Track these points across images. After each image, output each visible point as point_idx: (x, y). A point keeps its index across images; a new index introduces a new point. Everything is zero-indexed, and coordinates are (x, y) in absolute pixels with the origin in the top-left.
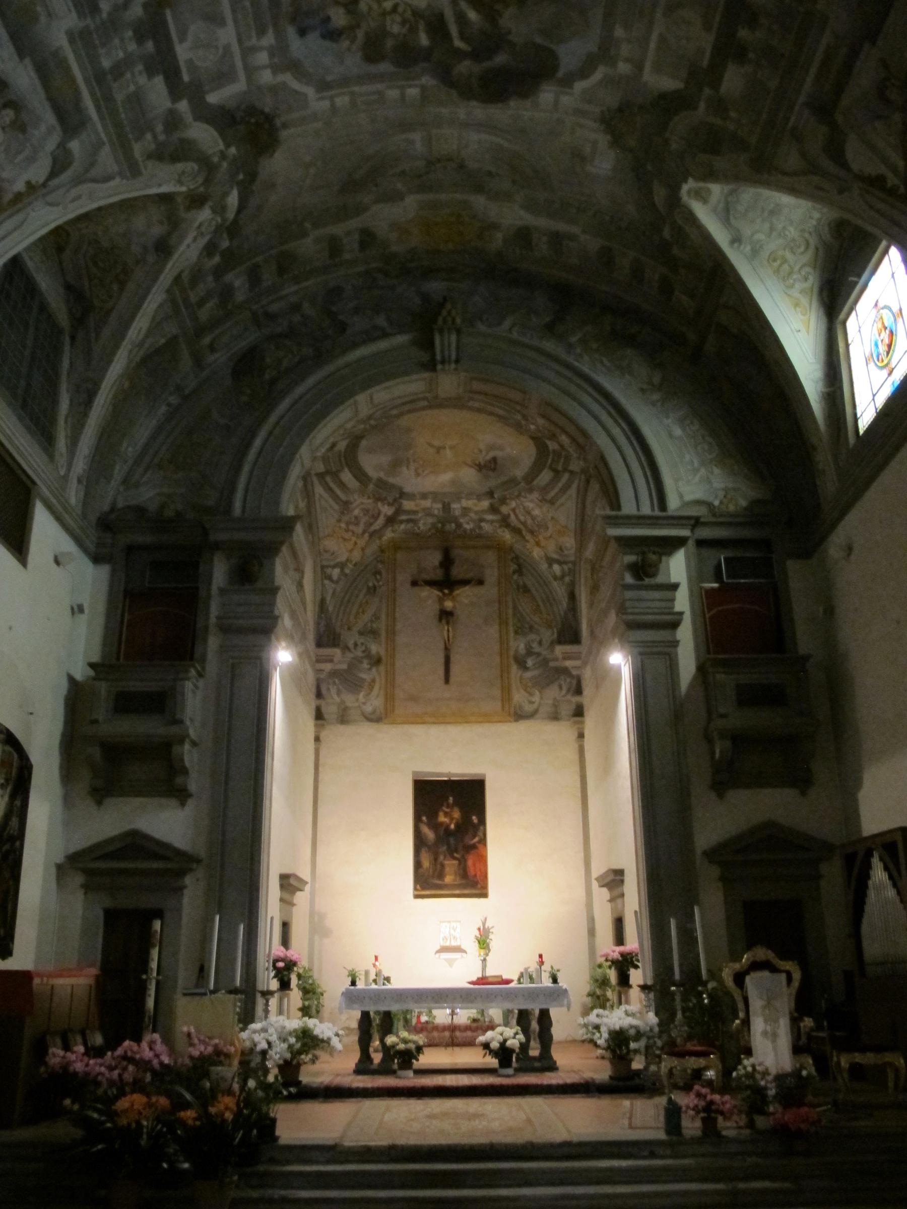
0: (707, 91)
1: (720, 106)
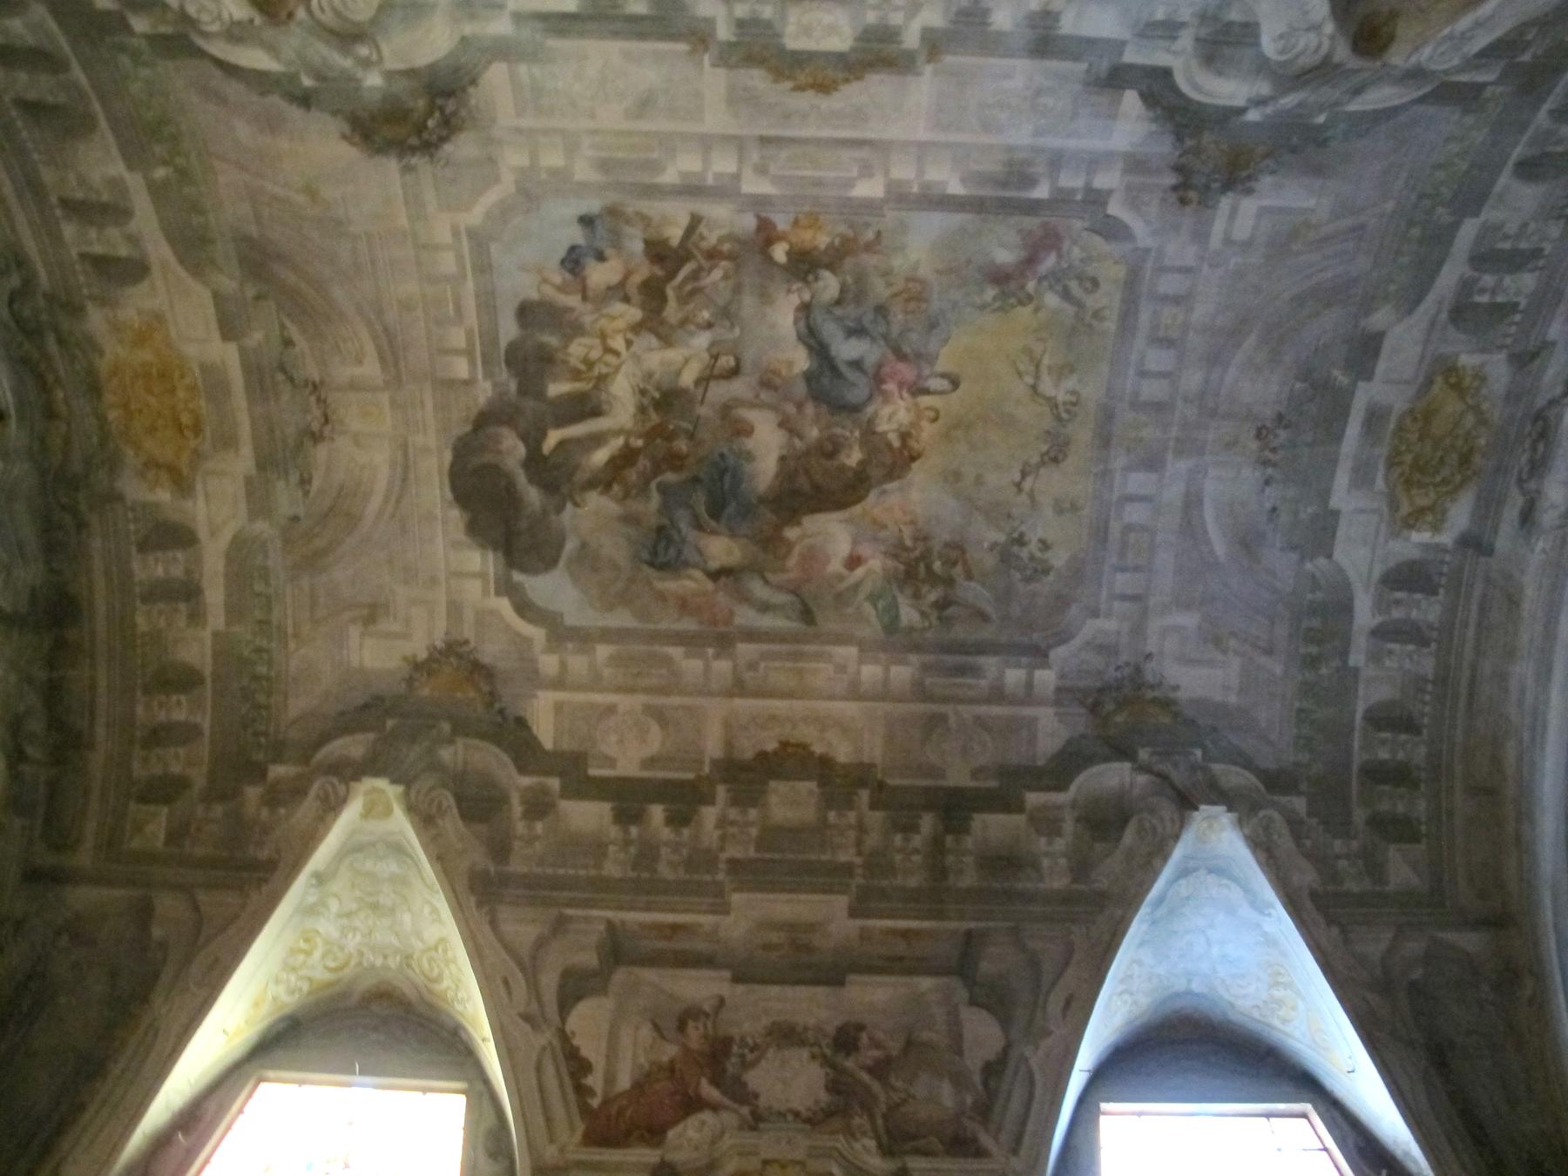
0: (554, 783)
1: (539, 807)
